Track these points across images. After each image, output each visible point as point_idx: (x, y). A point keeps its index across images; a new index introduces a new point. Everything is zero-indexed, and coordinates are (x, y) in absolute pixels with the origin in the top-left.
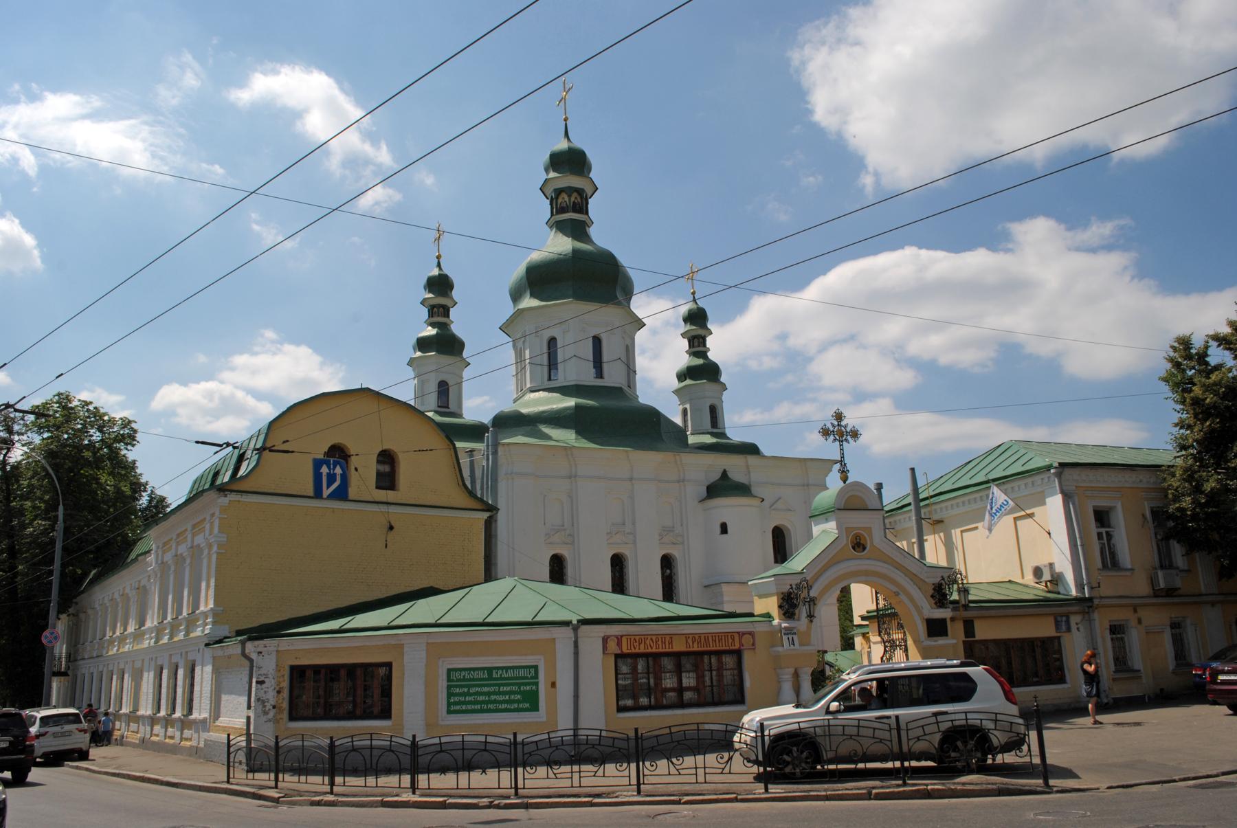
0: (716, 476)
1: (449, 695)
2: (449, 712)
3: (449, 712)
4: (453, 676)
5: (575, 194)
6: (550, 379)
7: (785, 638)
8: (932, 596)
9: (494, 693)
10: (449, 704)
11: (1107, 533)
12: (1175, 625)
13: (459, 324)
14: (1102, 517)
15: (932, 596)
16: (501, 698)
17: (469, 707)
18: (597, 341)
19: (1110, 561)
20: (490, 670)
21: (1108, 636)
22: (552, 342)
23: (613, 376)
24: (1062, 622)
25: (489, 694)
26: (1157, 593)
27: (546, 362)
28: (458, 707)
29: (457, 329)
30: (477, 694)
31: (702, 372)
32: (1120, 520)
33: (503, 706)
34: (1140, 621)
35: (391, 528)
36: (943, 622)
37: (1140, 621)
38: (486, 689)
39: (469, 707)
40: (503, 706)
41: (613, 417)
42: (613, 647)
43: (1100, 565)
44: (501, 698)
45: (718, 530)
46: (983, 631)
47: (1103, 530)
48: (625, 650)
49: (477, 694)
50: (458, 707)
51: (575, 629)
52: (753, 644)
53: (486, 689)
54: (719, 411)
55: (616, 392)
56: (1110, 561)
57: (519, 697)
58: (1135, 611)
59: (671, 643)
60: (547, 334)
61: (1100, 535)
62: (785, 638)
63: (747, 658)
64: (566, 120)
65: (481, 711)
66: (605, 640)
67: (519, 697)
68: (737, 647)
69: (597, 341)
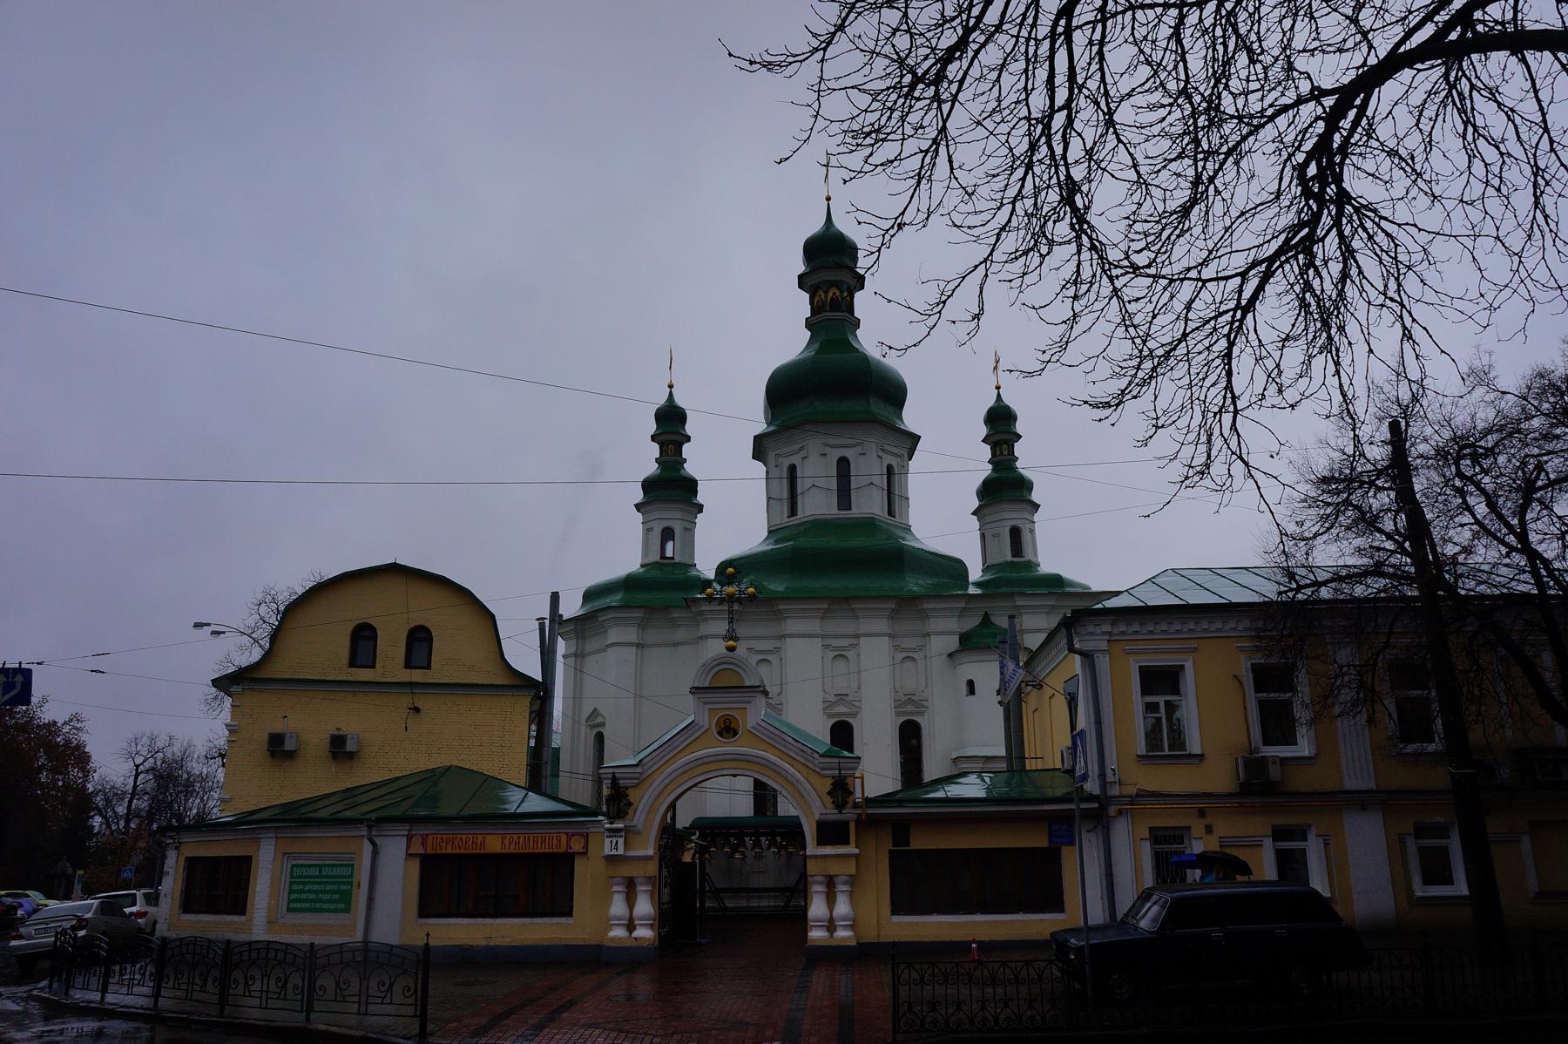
0: (971, 623)
1: (291, 892)
2: (289, 910)
3: (289, 910)
4: (297, 871)
5: (834, 290)
6: (793, 511)
7: (607, 841)
8: (829, 793)
9: (322, 892)
10: (290, 901)
11: (1167, 703)
12: (1279, 834)
13: (695, 460)
14: (1160, 680)
15: (829, 793)
16: (325, 897)
17: (304, 905)
18: (843, 463)
19: (1165, 741)
20: (320, 867)
21: (1146, 850)
22: (792, 468)
23: (868, 504)
24: (1063, 827)
25: (317, 892)
26: (1245, 789)
27: (785, 495)
28: (298, 905)
29: (690, 469)
30: (309, 892)
31: (1005, 489)
32: (1189, 681)
33: (326, 906)
34: (1209, 829)
35: (417, 710)
36: (845, 824)
37: (1209, 829)
38: (316, 887)
39: (304, 905)
40: (326, 906)
41: (840, 562)
42: (417, 849)
43: (1142, 750)
44: (325, 897)
45: (964, 688)
46: (921, 841)
47: (1161, 700)
48: (429, 851)
49: (309, 892)
50: (298, 905)
51: (370, 827)
52: (586, 846)
53: (316, 887)
54: (1026, 536)
55: (869, 524)
56: (1165, 741)
57: (337, 897)
58: (1202, 813)
59: (483, 844)
60: (786, 463)
61: (1151, 708)
62: (607, 841)
63: (579, 865)
64: (828, 199)
65: (322, 910)
66: (409, 839)
67: (337, 897)
68: (563, 849)
69: (843, 463)
